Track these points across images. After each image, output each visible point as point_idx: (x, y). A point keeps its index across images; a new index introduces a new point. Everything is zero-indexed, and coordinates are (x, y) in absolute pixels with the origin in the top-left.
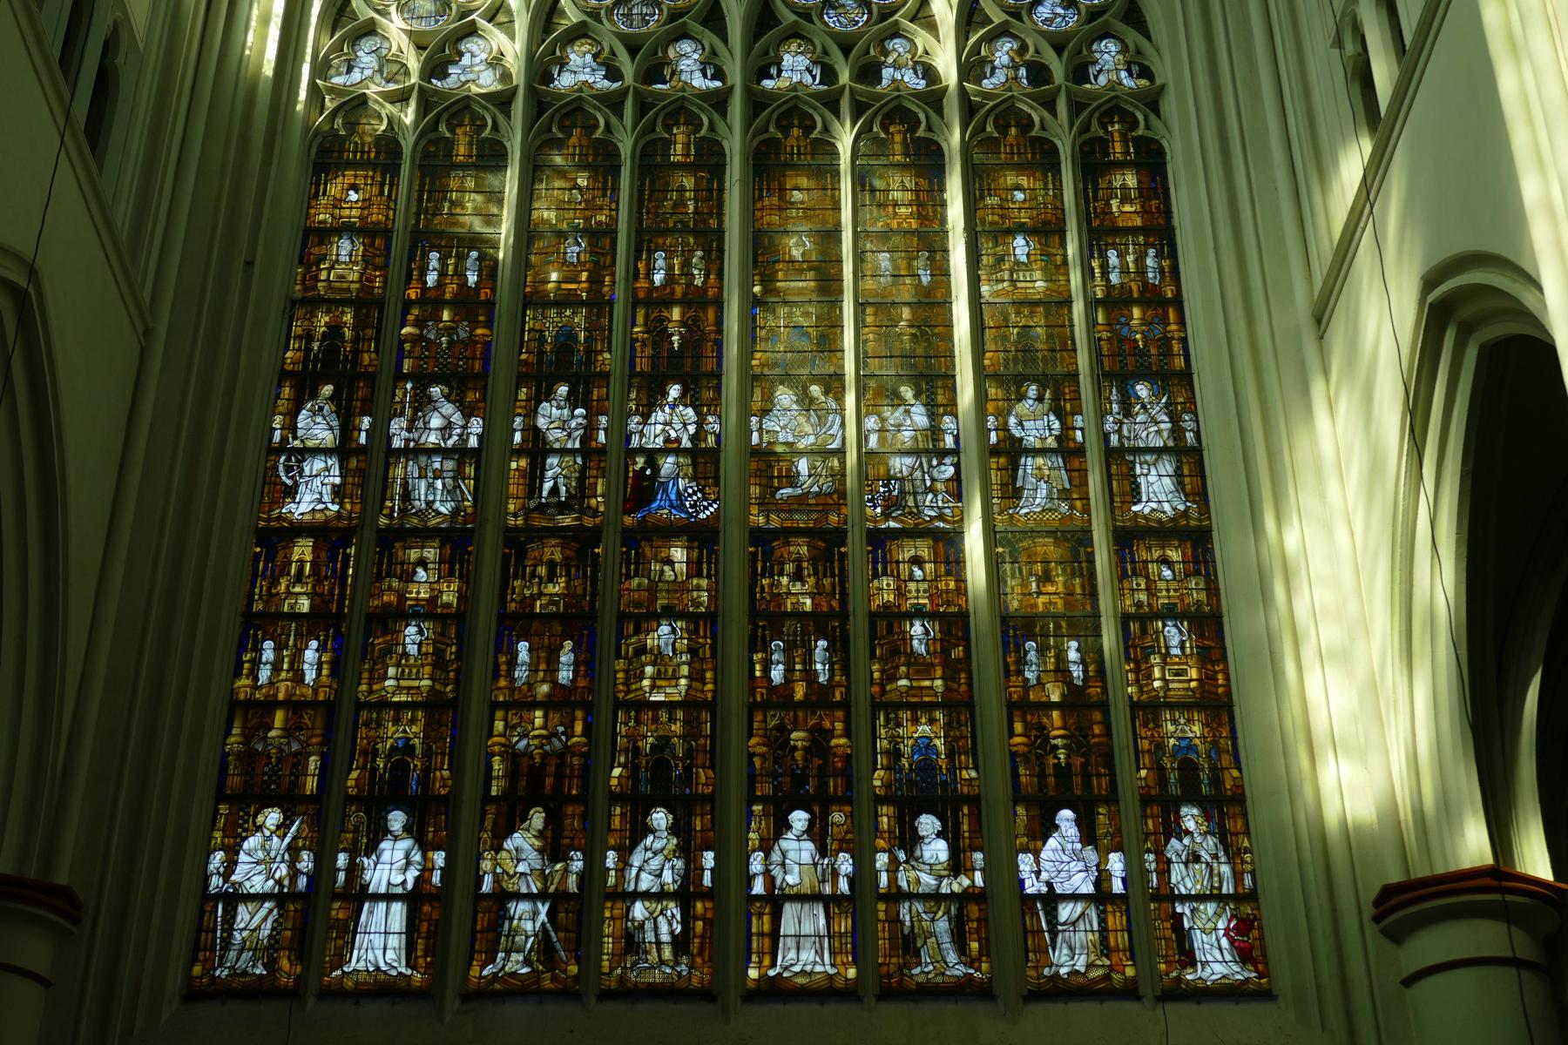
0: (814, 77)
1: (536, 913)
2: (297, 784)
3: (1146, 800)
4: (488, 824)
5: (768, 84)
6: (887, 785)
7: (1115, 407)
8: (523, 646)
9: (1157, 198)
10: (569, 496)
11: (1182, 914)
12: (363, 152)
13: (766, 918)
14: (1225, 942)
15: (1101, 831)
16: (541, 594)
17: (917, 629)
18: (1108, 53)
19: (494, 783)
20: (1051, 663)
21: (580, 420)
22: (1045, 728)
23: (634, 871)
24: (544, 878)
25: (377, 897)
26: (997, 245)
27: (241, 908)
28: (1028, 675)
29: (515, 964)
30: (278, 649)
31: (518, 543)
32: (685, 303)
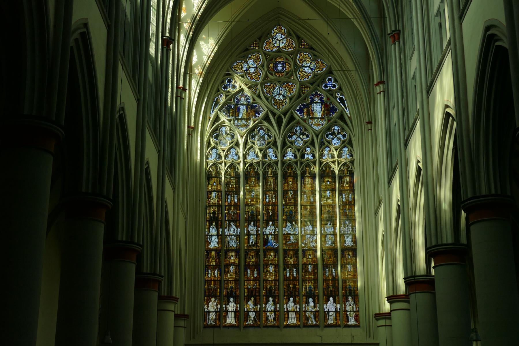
2: (216, 294)
3: (343, 296)
5: (285, 158)
8: (249, 270)
17: (310, 267)
24: (254, 309)
29: (251, 322)
30: (211, 271)
31: (247, 252)
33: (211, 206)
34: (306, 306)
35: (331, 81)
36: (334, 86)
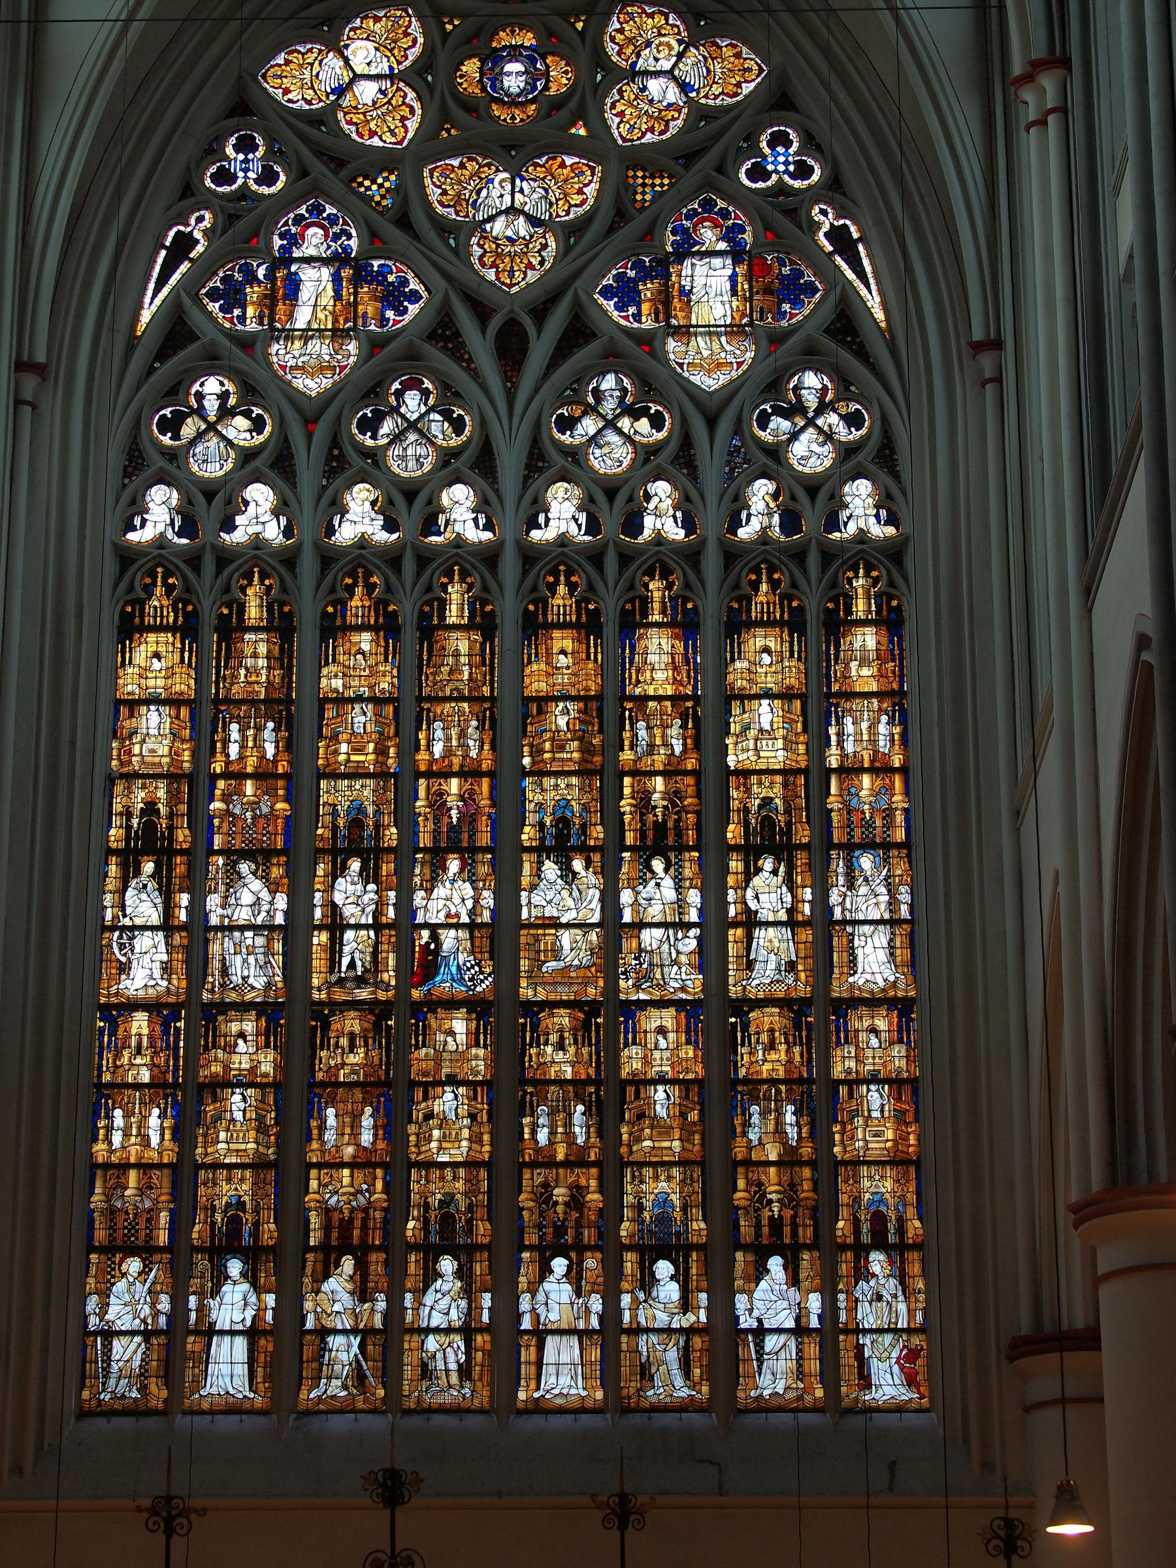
0: (580, 526)
1: (349, 1346)
4: (309, 1271)
5: (536, 535)
6: (631, 1236)
8: (331, 1112)
9: (893, 660)
10: (366, 971)
12: (162, 617)
13: (533, 1349)
14: (896, 1368)
15: (803, 1275)
16: (344, 1064)
18: (860, 496)
20: (771, 1127)
21: (372, 895)
23: (427, 1310)
25: (222, 1333)
27: (115, 1343)
28: (751, 1136)
29: (335, 1388)
30: (127, 1116)
31: (322, 1015)
32: (462, 774)
33: (136, 775)
35: (788, 144)
36: (803, 171)
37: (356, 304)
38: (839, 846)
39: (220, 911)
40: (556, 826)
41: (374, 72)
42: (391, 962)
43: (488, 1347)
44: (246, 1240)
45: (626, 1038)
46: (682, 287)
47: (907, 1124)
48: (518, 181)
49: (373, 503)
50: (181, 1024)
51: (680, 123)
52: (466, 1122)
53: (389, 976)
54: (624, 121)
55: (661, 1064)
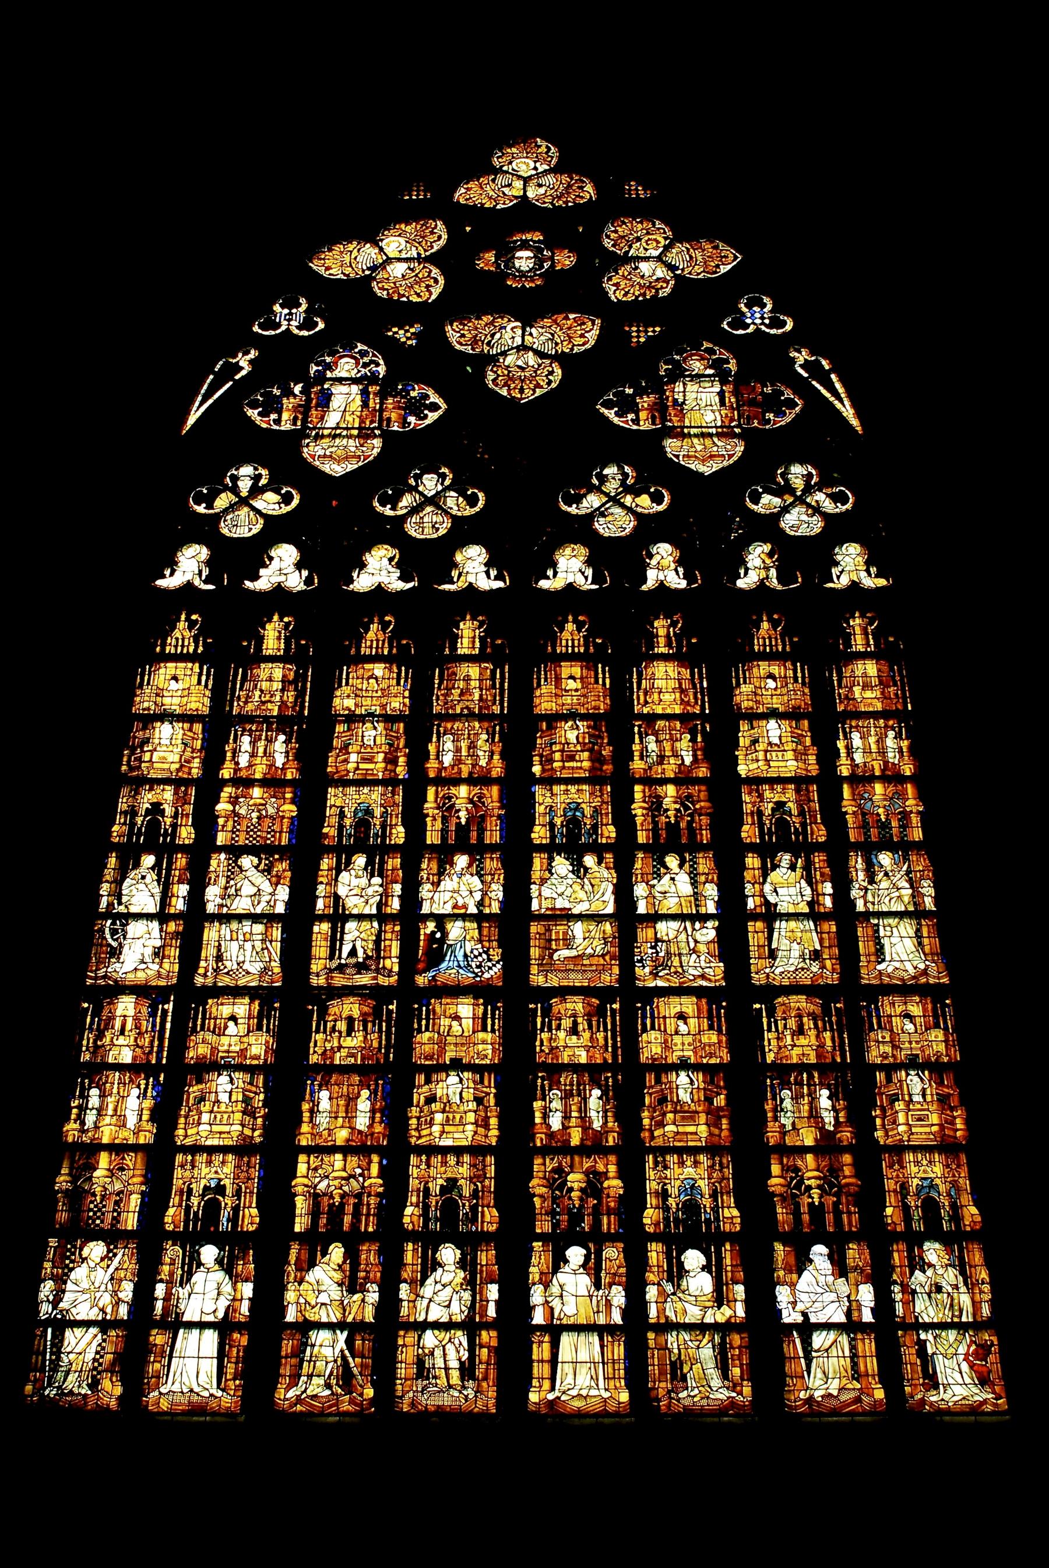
0: (586, 578)
1: (335, 1341)
7: (861, 875)
8: (324, 1095)
9: (895, 685)
10: (367, 957)
11: (925, 1341)
13: (546, 1346)
14: (965, 1367)
16: (340, 1047)
19: (297, 1220)
21: (377, 888)
22: (800, 1170)
23: (425, 1302)
25: (190, 1325)
26: (753, 728)
27: (68, 1333)
29: (316, 1387)
30: (103, 1096)
34: (663, 1294)
35: (763, 306)
37: (381, 410)
38: (857, 847)
39: (219, 901)
40: (567, 826)
41: (404, 256)
42: (395, 950)
43: (494, 1343)
44: (224, 1224)
45: (644, 1025)
46: (675, 401)
47: (952, 1109)
48: (528, 329)
49: (391, 560)
50: (170, 1007)
51: (668, 290)
52: (473, 1105)
53: (392, 963)
54: (617, 288)
55: (682, 1049)
